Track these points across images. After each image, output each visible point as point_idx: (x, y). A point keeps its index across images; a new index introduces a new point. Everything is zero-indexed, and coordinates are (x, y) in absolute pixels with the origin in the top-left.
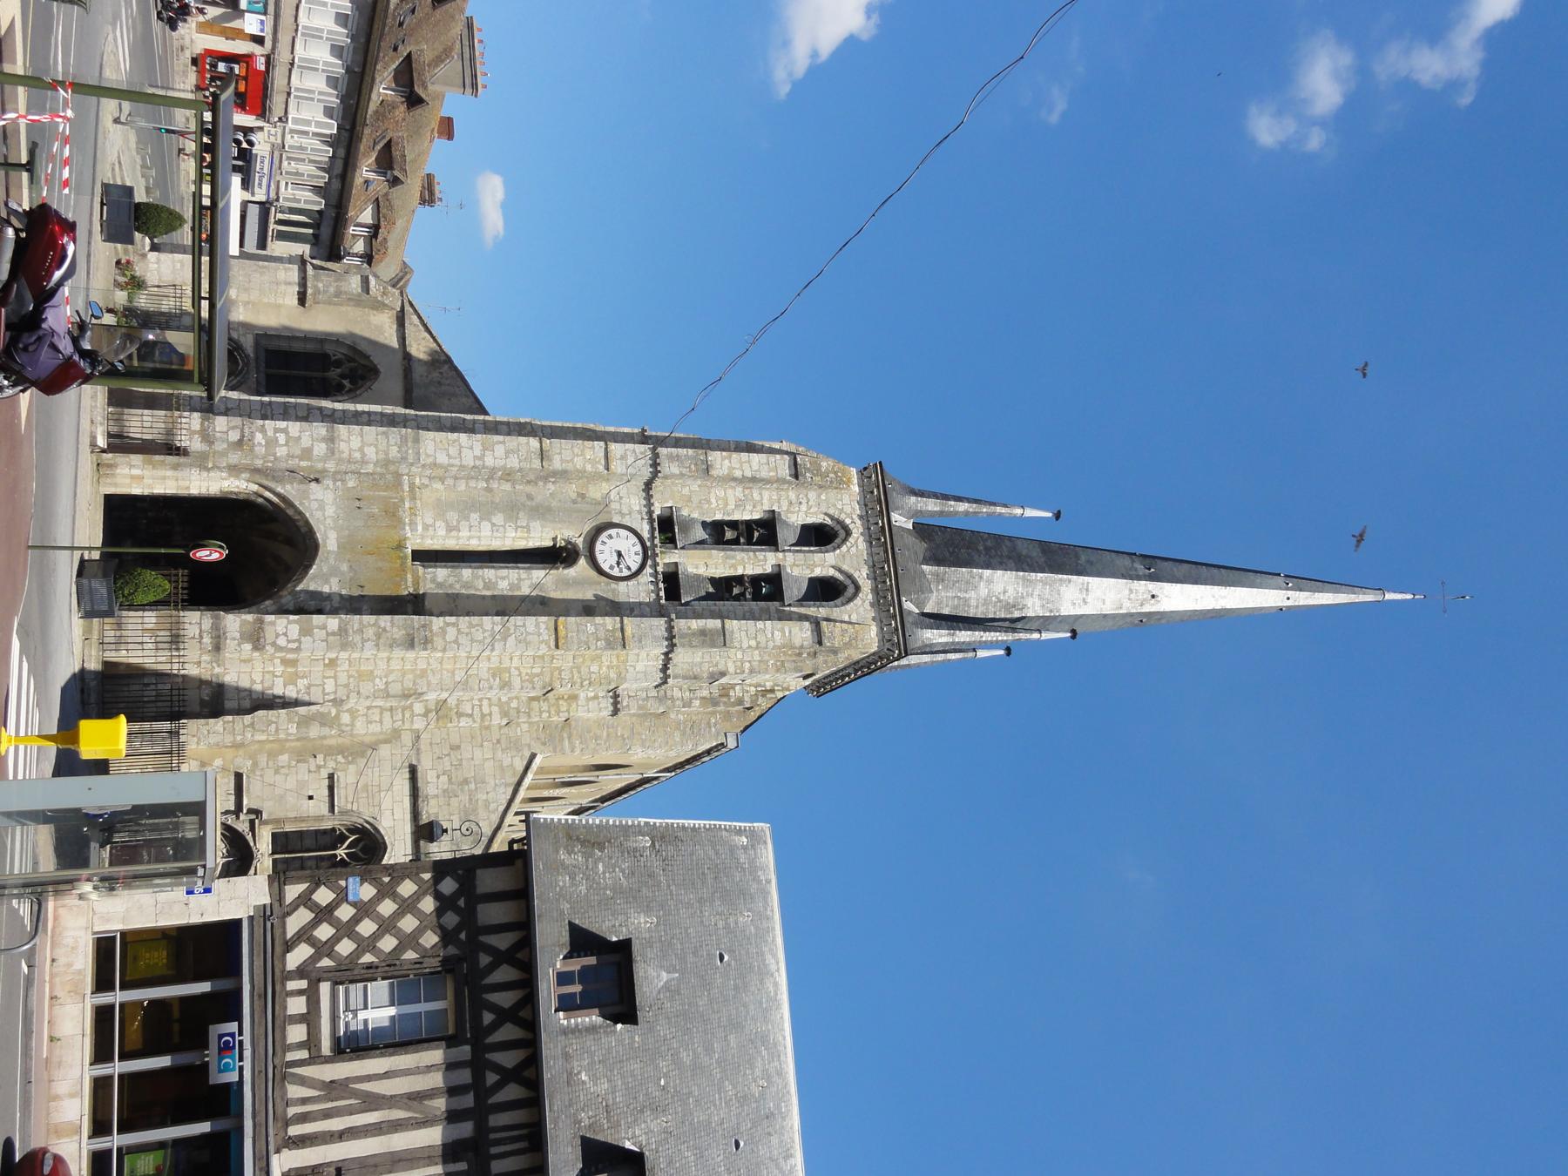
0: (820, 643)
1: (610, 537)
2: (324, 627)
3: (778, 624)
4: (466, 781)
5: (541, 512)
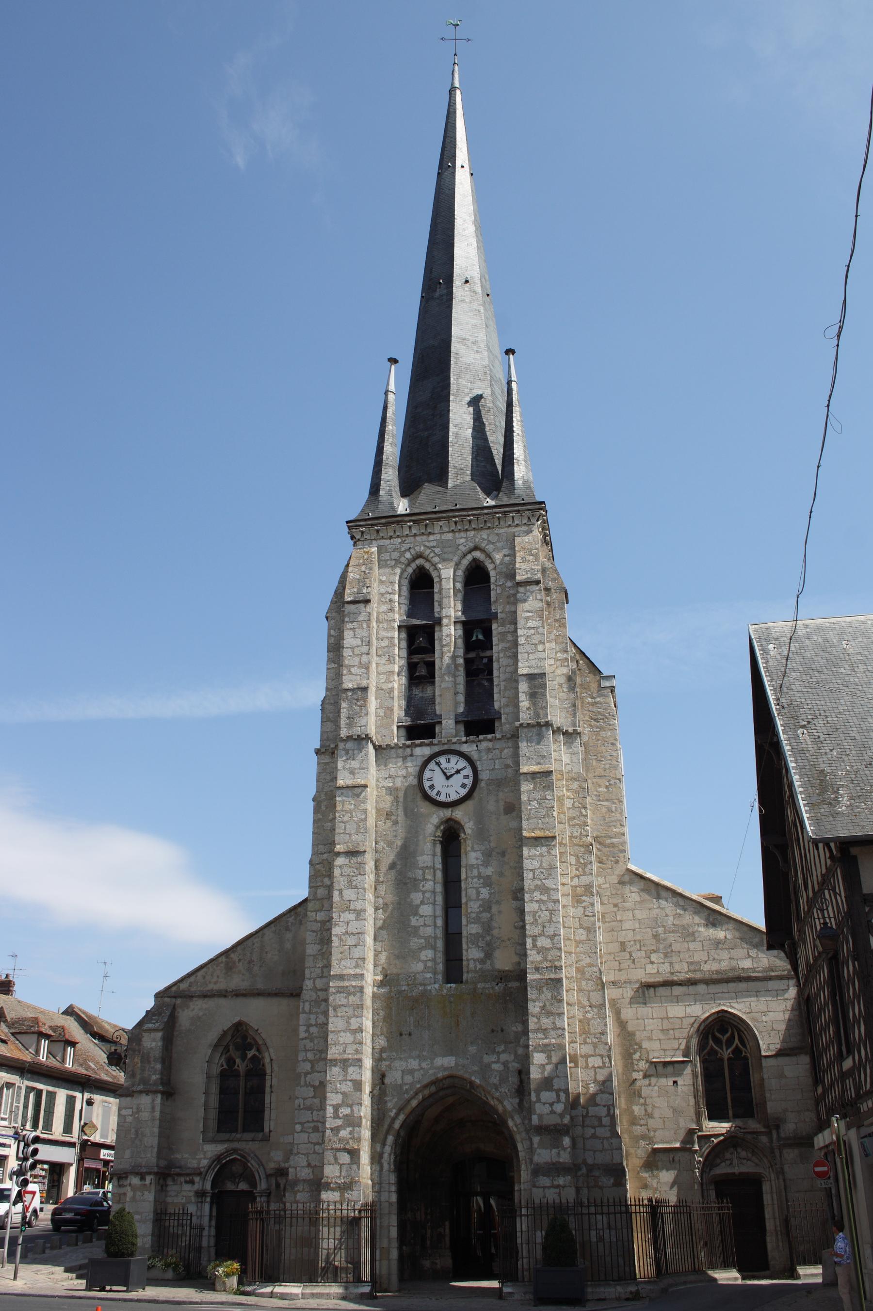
0: (538, 582)
1: (432, 787)
3: (521, 623)
4: (656, 936)
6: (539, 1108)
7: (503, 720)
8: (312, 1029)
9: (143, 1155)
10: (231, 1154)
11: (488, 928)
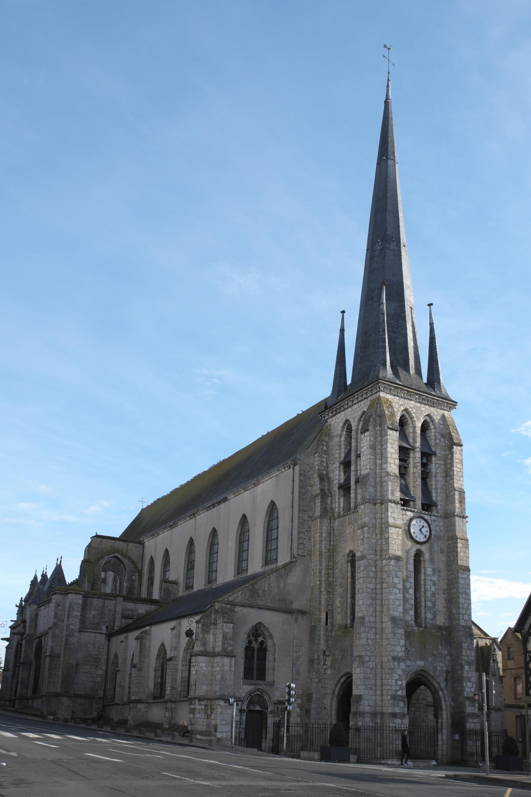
2: (468, 672)
6: (467, 690)
7: (439, 507)
8: (369, 641)
9: (226, 690)
10: (256, 692)
11: (434, 605)
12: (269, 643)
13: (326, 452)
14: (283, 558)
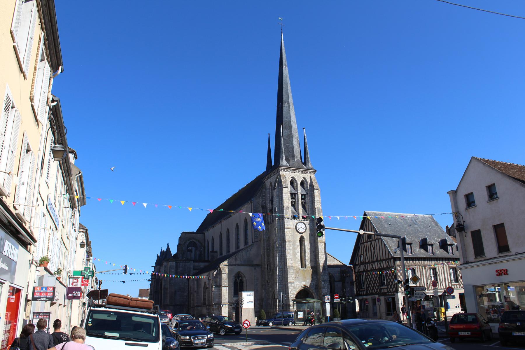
5: (295, 242)
6: (323, 292)
12: (244, 279)
13: (265, 196)
14: (250, 243)
